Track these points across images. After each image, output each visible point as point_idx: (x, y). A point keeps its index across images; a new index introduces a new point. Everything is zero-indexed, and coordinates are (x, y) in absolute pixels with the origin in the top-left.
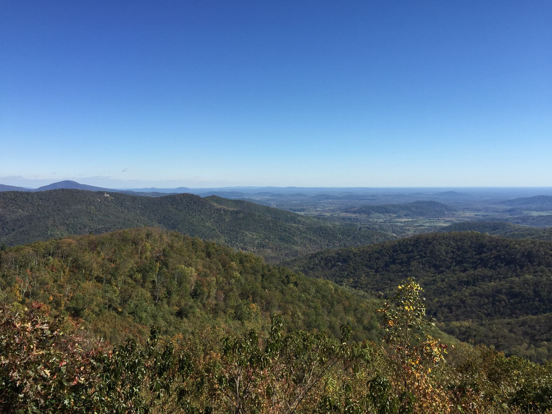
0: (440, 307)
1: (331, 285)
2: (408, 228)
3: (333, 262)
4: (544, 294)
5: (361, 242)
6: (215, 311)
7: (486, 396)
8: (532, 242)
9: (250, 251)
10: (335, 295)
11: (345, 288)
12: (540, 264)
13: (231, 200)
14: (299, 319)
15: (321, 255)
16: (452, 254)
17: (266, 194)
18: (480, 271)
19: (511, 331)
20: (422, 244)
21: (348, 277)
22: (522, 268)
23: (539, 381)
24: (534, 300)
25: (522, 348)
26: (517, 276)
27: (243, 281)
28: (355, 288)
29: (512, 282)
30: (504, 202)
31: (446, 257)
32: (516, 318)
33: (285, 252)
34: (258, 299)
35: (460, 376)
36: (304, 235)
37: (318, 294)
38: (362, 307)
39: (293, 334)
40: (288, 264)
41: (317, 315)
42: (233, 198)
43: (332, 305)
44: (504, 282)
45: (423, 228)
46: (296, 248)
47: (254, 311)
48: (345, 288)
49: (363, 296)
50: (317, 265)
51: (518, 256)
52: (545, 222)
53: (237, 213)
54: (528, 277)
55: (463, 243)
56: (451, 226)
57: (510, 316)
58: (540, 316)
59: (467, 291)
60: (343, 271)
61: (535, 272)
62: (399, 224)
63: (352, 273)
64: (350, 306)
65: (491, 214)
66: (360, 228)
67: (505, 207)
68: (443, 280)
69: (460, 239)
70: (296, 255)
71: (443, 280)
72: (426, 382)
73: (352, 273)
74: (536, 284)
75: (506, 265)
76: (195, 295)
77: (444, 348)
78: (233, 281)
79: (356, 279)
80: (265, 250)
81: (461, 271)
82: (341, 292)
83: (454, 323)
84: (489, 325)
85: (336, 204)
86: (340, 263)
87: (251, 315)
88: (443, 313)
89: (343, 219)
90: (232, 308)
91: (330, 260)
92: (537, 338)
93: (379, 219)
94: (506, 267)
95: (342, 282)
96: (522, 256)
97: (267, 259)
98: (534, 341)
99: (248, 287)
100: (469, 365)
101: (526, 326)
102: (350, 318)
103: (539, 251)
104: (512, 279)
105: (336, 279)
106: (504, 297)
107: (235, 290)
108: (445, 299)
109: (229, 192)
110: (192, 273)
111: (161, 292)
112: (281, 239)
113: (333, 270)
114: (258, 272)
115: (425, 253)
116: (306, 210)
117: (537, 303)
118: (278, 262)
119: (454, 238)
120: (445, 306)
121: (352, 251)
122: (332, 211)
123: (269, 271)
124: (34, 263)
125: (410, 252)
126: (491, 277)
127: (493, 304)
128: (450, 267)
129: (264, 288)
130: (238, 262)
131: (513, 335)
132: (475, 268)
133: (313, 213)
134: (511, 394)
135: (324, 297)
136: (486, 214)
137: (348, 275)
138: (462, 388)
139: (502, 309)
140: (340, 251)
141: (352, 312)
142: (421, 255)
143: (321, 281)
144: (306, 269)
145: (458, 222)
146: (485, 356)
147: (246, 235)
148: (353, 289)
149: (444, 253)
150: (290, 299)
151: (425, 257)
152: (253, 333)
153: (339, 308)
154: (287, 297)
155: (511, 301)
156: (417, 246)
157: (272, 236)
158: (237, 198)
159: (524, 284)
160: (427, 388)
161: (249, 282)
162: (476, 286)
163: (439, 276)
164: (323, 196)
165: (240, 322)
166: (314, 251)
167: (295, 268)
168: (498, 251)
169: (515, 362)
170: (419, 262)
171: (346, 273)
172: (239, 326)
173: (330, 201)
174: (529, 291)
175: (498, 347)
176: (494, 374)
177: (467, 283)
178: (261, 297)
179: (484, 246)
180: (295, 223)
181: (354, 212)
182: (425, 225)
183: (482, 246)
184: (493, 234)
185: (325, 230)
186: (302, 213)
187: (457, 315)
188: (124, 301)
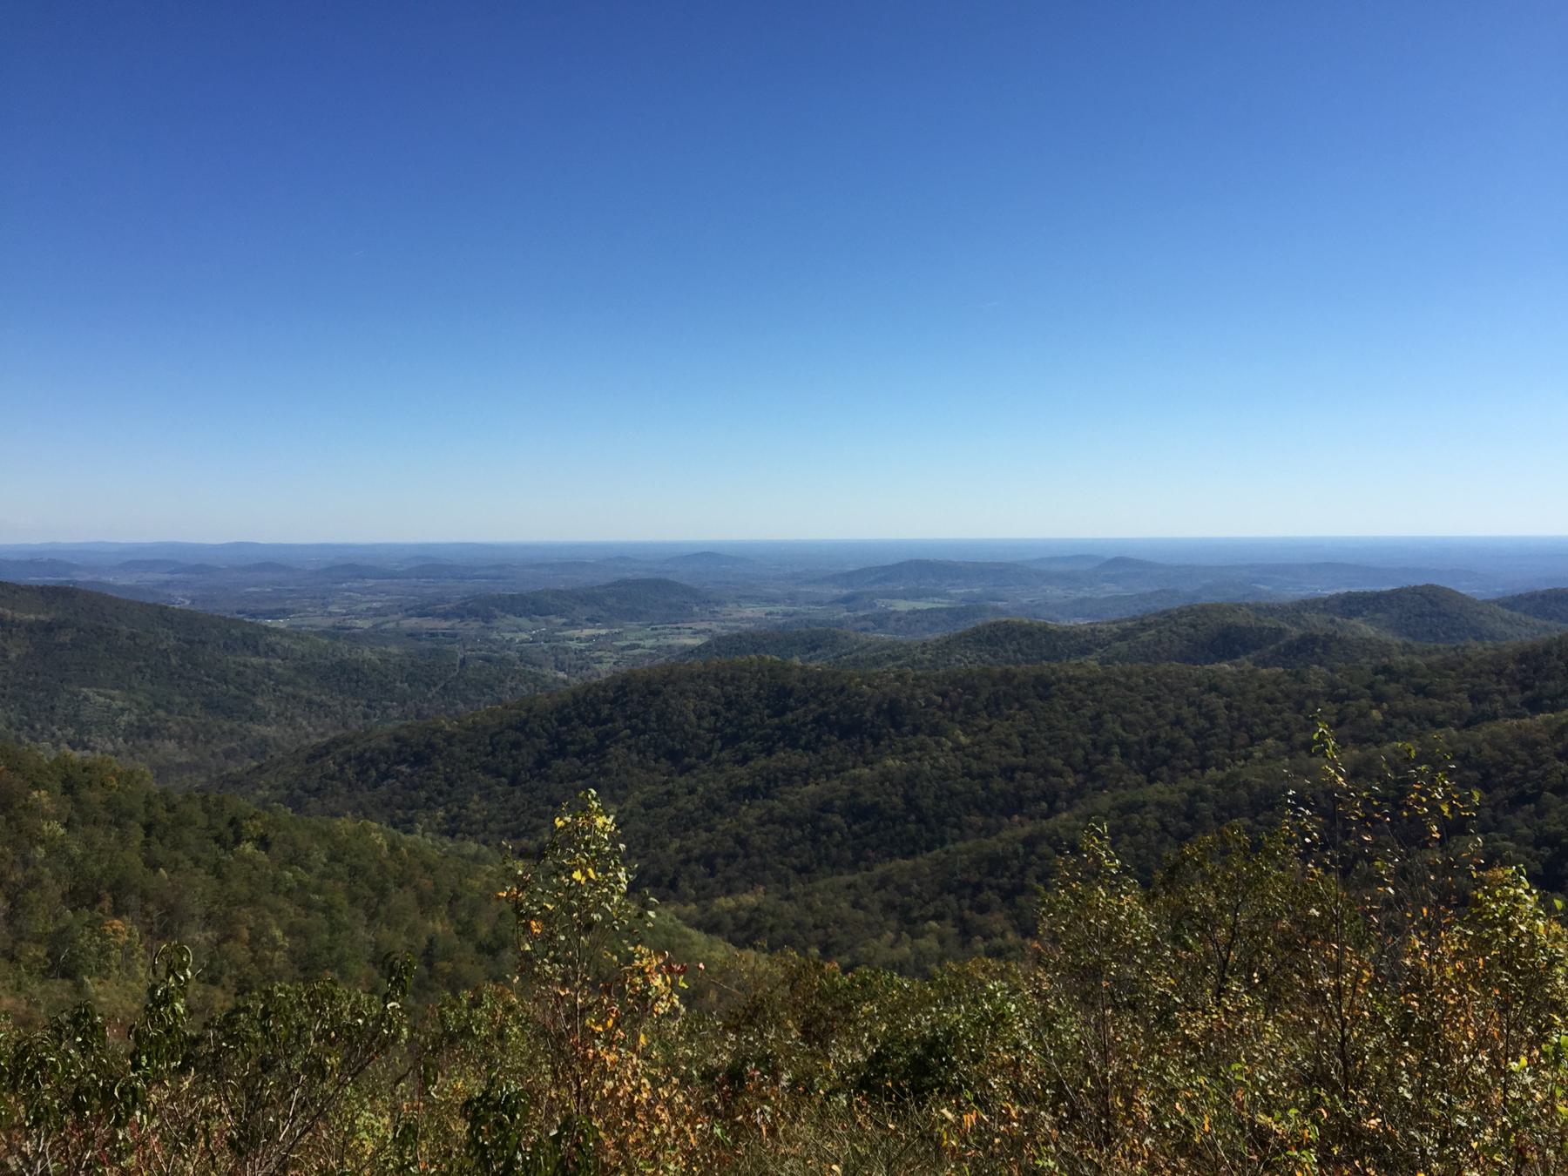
0: (686, 862)
1: (379, 835)
2: (599, 653)
3: (383, 766)
4: (927, 802)
5: (466, 701)
7: (794, 1083)
8: (899, 677)
9: (102, 750)
10: (390, 864)
11: (423, 840)
12: (916, 730)
13: (29, 589)
14: (276, 948)
15: (347, 748)
16: (713, 718)
17: (152, 565)
18: (785, 758)
19: (855, 905)
20: (636, 697)
21: (429, 805)
22: (876, 741)
23: (918, 1024)
24: (907, 822)
25: (882, 946)
26: (867, 763)
27: (76, 850)
28: (453, 836)
29: (856, 780)
30: (833, 579)
31: (699, 727)
32: (867, 869)
33: (225, 746)
34: (133, 901)
35: (731, 1043)
36: (289, 689)
37: (338, 868)
38: (472, 889)
39: (253, 998)
40: (237, 782)
41: (335, 929)
42: (34, 580)
43: (382, 893)
44: (837, 783)
45: (637, 652)
46: (270, 731)
47: (120, 942)
48: (423, 840)
49: (476, 858)
50: (332, 778)
51: (868, 714)
52: (926, 625)
53: (49, 628)
55: (738, 688)
56: (708, 645)
57: (854, 866)
58: (920, 860)
59: (751, 813)
60: (415, 789)
61: (907, 750)
62: (574, 645)
63: (440, 793)
64: (437, 891)
65: (803, 609)
66: (463, 662)
67: (835, 591)
68: (692, 791)
69: (733, 678)
70: (263, 753)
71: (692, 791)
72: (635, 1073)
73: (440, 793)
74: (911, 780)
75: (840, 739)
77: (679, 973)
78: (41, 852)
79: (456, 809)
80: (157, 744)
81: (736, 762)
82: (410, 852)
83: (722, 901)
84: (805, 894)
85: (388, 593)
86: (404, 768)
87: (108, 958)
88: (692, 877)
89: (414, 635)
90: (39, 942)
91: (372, 761)
92: (915, 914)
93: (516, 632)
94: (842, 744)
95: (410, 821)
96: (878, 714)
97: (161, 772)
98: (910, 924)
99: (96, 869)
100: (757, 1009)
101: (890, 888)
102: (439, 926)
103: (912, 697)
104: (857, 771)
105: (392, 817)
106: (837, 819)
107: (46, 881)
108: (698, 840)
109: (18, 562)
112: (211, 706)
113: (383, 788)
114: (131, 816)
115: (645, 722)
116: (293, 612)
117: (912, 827)
118: (203, 780)
119: (716, 675)
120: (697, 860)
121: (440, 730)
122: (378, 613)
123: (171, 809)
125: (605, 722)
126: (807, 771)
127: (815, 840)
128: (709, 754)
129: (153, 865)
130: (58, 788)
131: (861, 914)
132: (770, 752)
133: (317, 620)
134: (855, 1068)
135: (354, 871)
136: (791, 609)
137: (428, 799)
138: (735, 1075)
139: (834, 851)
140: (403, 732)
141: (444, 908)
142: (633, 728)
143: (345, 825)
144: (298, 792)
145: (725, 632)
146: (793, 980)
147: (86, 698)
148: (446, 839)
149: (693, 718)
150: (244, 891)
151: (644, 732)
152: (86, 1015)
153: (402, 899)
154: (235, 885)
155: (855, 828)
156: (624, 704)
157: (178, 699)
158: (50, 580)
159: (882, 784)
160: (637, 1090)
161: (101, 851)
162: (773, 798)
163: (682, 780)
164: (348, 570)
165: (68, 983)
166: (323, 735)
167: (260, 792)
168: (823, 704)
169: (864, 984)
170: (629, 748)
171: (423, 794)
172: (65, 995)
173: (370, 582)
174: (895, 799)
175: (827, 951)
176: (817, 1021)
177: (752, 793)
178: (145, 896)
179: (790, 693)
180: (257, 654)
181: (445, 616)
182: (611, 649)
183: (784, 693)
184: (810, 660)
185: (357, 670)
186: (281, 623)
187: (728, 880)
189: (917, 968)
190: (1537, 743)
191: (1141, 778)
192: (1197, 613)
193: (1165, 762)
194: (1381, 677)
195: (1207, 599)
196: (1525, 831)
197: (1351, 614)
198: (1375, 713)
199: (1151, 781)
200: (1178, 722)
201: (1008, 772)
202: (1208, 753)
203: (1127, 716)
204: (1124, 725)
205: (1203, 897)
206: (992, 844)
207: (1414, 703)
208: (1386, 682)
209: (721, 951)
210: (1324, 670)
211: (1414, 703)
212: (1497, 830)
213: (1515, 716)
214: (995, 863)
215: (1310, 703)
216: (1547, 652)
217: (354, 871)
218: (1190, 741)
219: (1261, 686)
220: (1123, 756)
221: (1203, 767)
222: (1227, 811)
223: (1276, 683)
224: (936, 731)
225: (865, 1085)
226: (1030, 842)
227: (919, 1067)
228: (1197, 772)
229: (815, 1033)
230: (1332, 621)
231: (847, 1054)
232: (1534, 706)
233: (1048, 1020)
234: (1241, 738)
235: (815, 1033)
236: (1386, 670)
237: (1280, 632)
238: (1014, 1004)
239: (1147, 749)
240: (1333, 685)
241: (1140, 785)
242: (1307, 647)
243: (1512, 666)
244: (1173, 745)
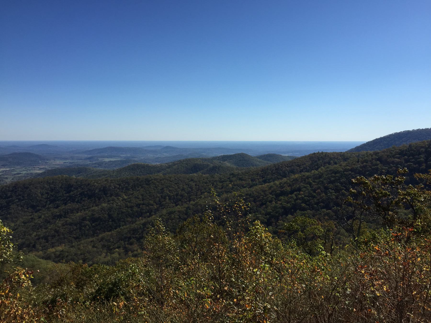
0: (38, 239)
2: (7, 176)
7: (72, 301)
8: (106, 180)
12: (111, 195)
16: (46, 195)
18: (70, 206)
19: (93, 247)
20: (20, 189)
22: (99, 200)
23: (111, 278)
24: (109, 221)
25: (102, 258)
26: (97, 205)
29: (93, 210)
31: (42, 198)
32: (97, 236)
35: (52, 292)
44: (87, 212)
45: (20, 175)
51: (97, 191)
52: (114, 165)
54: (104, 205)
55: (55, 185)
56: (45, 172)
57: (93, 236)
58: (113, 232)
59: (59, 223)
61: (109, 201)
65: (76, 161)
67: (86, 156)
68: (40, 217)
69: (53, 182)
71: (40, 217)
72: (16, 306)
75: (88, 199)
77: (31, 274)
81: (55, 208)
83: (51, 249)
84: (78, 245)
88: (41, 243)
92: (112, 247)
94: (89, 201)
96: (100, 191)
98: (110, 250)
100: (62, 281)
101: (104, 241)
103: (110, 186)
104: (93, 208)
106: (88, 222)
108: (42, 232)
115: (23, 197)
117: (110, 223)
119: (47, 182)
120: (42, 238)
125: (9, 197)
126: (78, 209)
127: (80, 229)
128: (45, 206)
131: (95, 249)
132: (66, 204)
134: (92, 294)
136: (72, 161)
138: (54, 301)
139: (87, 232)
142: (19, 199)
145: (50, 169)
146: (73, 271)
149: (40, 195)
151: (23, 200)
155: (93, 224)
156: (16, 192)
159: (101, 211)
160: (17, 311)
162: (67, 218)
163: (36, 214)
168: (83, 189)
169: (95, 269)
170: (18, 205)
174: (105, 215)
175: (84, 261)
176: (81, 281)
177: (60, 216)
179: (72, 186)
184: (78, 176)
187: (53, 243)
189: (113, 263)
190: (266, 191)
191: (174, 205)
192: (188, 161)
193: (180, 200)
194: (231, 176)
195: (190, 157)
196: (263, 212)
197: (224, 161)
198: (230, 185)
199: (176, 205)
200: (183, 190)
201: (138, 205)
202: (191, 197)
203: (170, 189)
204: (169, 191)
205: (188, 235)
206: (134, 226)
207: (239, 182)
208: (233, 177)
209: (50, 264)
210: (218, 174)
211: (239, 182)
212: (257, 212)
213: (261, 184)
214: (135, 231)
215: (215, 183)
216: (267, 169)
218: (186, 194)
219: (204, 179)
220: (169, 199)
221: (190, 201)
222: (197, 211)
223: (207, 178)
224: (117, 195)
225: (94, 299)
226: (144, 224)
227: (111, 291)
228: (188, 202)
229: (80, 286)
230: (220, 162)
231: (90, 290)
232: (265, 182)
233: (147, 273)
234: (199, 193)
235: (80, 286)
236: (232, 174)
237: (208, 165)
238: (138, 270)
239: (175, 197)
240: (220, 179)
241: (174, 207)
242: (215, 169)
243: (260, 172)
244: (182, 196)
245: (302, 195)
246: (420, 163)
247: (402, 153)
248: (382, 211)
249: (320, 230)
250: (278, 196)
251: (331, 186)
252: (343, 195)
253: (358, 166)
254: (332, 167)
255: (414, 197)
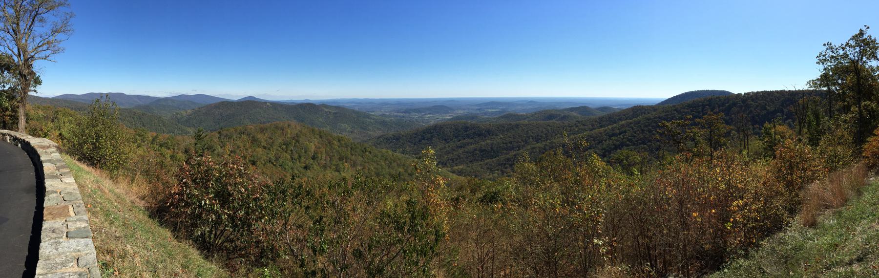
1: (390, 152)
4: (495, 149)
6: (325, 167)
18: (467, 140)
30: (477, 105)
48: (398, 154)
54: (488, 141)
59: (460, 151)
74: (492, 144)
76: (314, 158)
93: (415, 116)
98: (492, 171)
102: (401, 170)
110: (312, 147)
111: (296, 156)
124: (235, 137)
143: (384, 150)
146: (469, 182)
153: (395, 164)
175: (476, 177)
177: (461, 147)
183: (467, 128)
188: (277, 159)
189: (494, 180)
201: (511, 142)
206: (508, 156)
209: (455, 176)
214: (508, 159)
217: (386, 159)
224: (497, 135)
225: (482, 201)
226: (515, 155)
227: (493, 197)
229: (473, 191)
231: (479, 195)
232: (601, 127)
233: (517, 188)
235: (473, 191)
238: (510, 185)
242: (564, 118)
245: (627, 135)
246: (699, 112)
247: (689, 106)
248: (675, 142)
249: (638, 159)
250: (610, 136)
251: (646, 129)
252: (654, 135)
253: (663, 115)
254: (646, 116)
255: (695, 134)
